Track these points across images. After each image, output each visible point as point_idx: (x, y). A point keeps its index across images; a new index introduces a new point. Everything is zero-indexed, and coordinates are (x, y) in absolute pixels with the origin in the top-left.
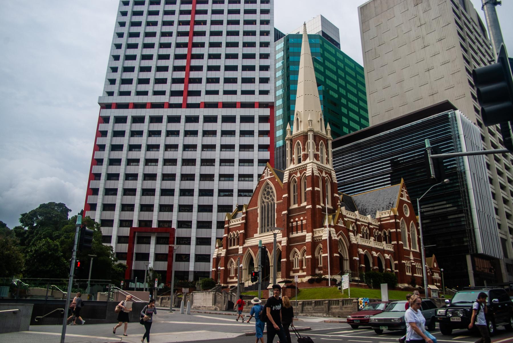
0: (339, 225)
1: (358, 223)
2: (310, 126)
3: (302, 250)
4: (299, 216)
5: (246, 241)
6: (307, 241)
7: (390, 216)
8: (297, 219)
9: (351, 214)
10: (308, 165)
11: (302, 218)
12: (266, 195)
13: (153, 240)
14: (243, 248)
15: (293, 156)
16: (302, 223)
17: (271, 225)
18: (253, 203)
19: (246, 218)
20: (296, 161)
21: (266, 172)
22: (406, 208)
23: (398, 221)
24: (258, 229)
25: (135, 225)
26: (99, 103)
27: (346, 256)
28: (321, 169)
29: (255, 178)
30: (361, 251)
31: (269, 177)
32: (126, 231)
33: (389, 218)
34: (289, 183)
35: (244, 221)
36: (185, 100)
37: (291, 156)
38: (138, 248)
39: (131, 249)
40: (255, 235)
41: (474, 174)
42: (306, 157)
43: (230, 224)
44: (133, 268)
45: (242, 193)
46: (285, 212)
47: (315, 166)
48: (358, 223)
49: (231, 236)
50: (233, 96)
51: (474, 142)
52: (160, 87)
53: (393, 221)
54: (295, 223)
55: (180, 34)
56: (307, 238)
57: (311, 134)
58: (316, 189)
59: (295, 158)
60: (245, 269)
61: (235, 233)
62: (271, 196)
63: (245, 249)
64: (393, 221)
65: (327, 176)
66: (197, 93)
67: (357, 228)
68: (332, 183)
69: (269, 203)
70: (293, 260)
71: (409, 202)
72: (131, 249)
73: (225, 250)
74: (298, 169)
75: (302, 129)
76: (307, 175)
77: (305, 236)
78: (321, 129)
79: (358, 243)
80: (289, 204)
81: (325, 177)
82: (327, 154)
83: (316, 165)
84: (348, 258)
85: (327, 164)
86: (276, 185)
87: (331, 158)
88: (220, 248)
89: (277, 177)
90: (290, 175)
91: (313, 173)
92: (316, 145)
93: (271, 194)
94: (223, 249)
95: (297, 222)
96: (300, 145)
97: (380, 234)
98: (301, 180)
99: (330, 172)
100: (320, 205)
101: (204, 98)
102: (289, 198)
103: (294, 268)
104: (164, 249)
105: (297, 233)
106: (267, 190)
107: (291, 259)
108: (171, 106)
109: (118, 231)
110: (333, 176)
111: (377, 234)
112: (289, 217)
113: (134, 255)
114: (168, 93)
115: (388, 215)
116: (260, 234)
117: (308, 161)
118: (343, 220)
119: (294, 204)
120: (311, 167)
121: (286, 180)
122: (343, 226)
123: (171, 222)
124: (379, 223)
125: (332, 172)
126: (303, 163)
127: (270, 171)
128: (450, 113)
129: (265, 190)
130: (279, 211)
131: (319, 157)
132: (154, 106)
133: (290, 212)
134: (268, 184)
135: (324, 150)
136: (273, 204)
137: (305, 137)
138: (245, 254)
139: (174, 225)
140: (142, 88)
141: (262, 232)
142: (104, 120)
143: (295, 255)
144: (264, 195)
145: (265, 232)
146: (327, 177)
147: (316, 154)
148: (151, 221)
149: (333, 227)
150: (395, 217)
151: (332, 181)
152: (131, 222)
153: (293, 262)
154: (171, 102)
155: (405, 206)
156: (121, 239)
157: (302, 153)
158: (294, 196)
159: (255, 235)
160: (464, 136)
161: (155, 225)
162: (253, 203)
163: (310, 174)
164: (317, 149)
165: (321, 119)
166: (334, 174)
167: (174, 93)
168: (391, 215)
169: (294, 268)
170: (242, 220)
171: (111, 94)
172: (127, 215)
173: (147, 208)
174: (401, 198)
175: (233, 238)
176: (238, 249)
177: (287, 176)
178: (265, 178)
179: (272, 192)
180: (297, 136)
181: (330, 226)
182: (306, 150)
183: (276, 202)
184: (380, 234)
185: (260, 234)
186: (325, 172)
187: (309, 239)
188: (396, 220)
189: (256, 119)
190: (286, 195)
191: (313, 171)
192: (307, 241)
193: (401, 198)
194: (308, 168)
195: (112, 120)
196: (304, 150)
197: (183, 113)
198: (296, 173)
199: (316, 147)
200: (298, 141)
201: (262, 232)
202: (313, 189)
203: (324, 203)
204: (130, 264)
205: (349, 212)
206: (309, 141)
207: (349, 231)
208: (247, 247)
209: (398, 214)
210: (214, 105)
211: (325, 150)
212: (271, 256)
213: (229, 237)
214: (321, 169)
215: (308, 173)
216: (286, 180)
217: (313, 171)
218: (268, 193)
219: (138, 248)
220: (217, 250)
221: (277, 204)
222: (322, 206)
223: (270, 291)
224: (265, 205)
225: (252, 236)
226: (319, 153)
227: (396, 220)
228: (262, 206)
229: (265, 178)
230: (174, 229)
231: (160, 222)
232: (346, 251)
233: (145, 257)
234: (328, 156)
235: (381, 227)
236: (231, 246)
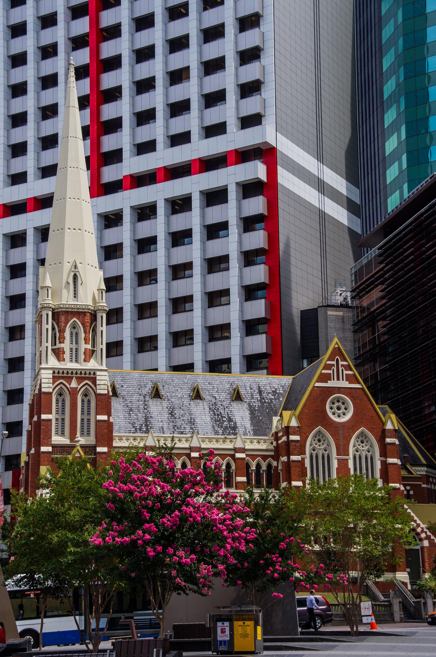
2: (50, 298)
65: (87, 384)
92: (59, 331)
99: (94, 374)
131: (64, 353)
147: (59, 349)
164: (59, 339)
184: (277, 467)
211: (83, 335)
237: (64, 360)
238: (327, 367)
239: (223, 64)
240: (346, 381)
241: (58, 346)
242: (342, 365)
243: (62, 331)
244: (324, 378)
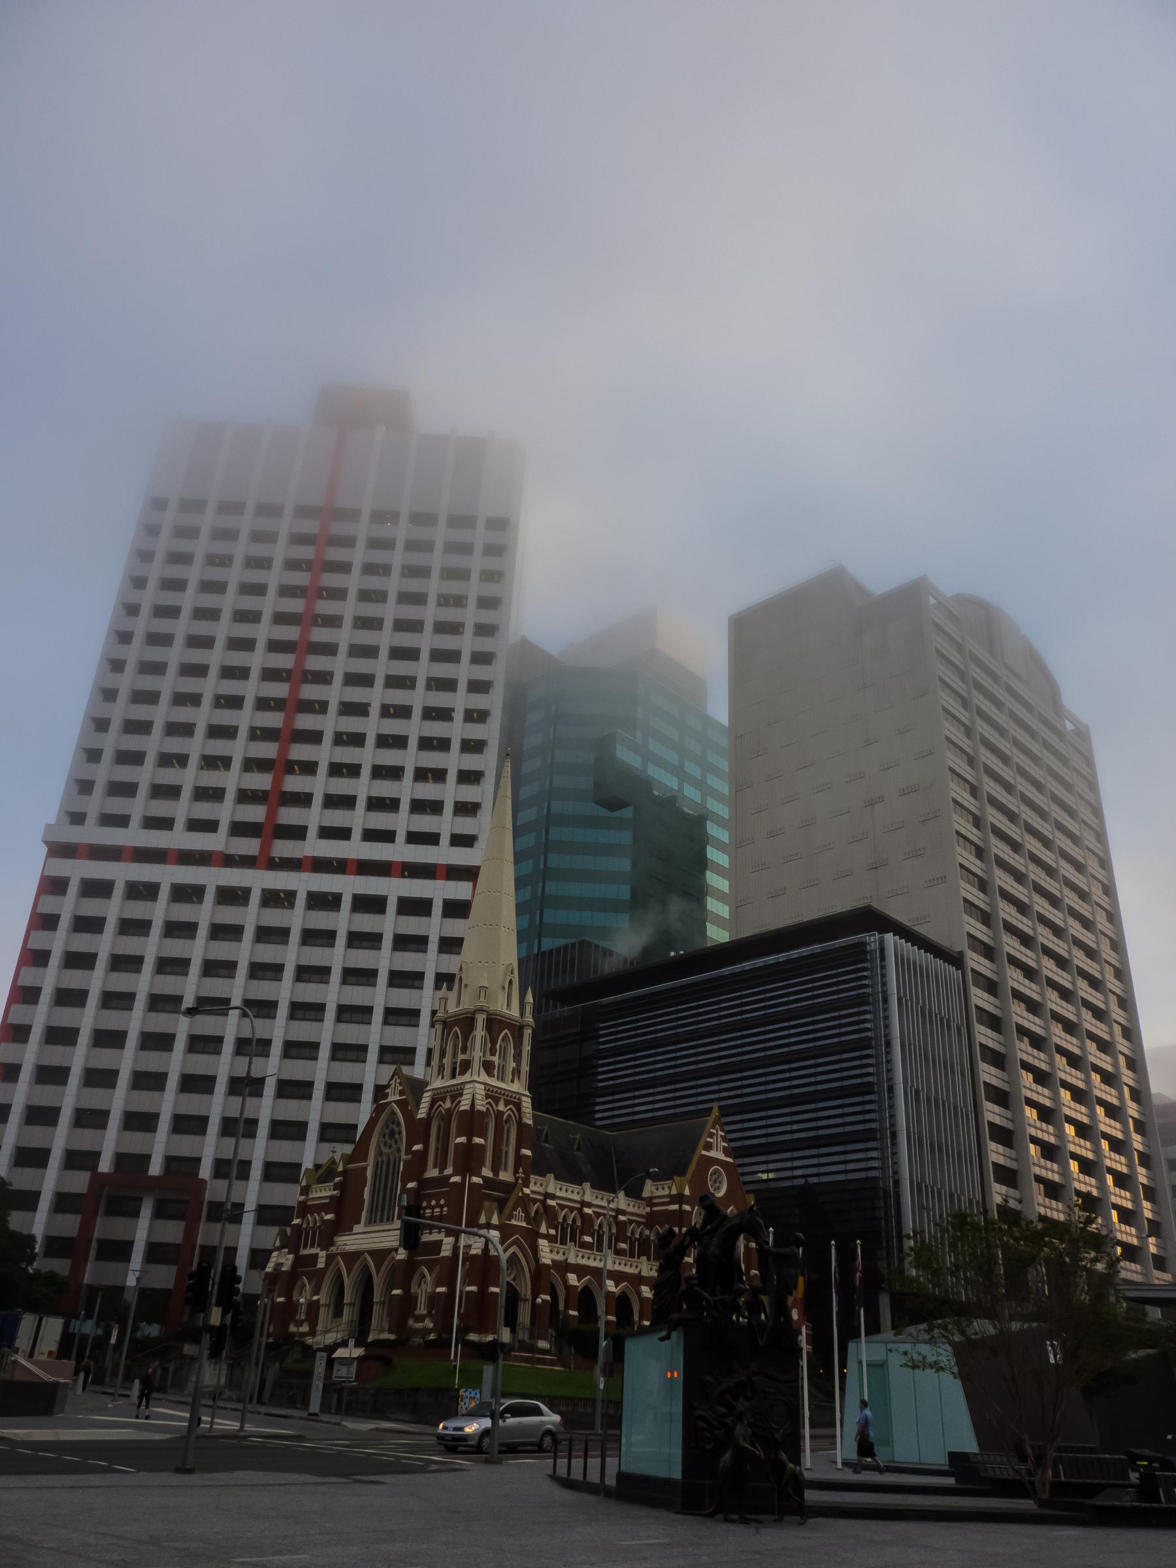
0: (513, 1222)
1: (587, 1210)
2: (482, 999)
4: (437, 1197)
5: (336, 1239)
6: (443, 1254)
7: (669, 1196)
8: (433, 1203)
9: (570, 1189)
10: (467, 1086)
11: (442, 1202)
12: (387, 1137)
13: (146, 1211)
14: (327, 1255)
15: (445, 1061)
16: (441, 1212)
17: (390, 1205)
18: (360, 1153)
20: (447, 1071)
21: (393, 1086)
22: (720, 1175)
23: (687, 1208)
24: (364, 1214)
25: (105, 1165)
26: (46, 842)
27: (526, 1290)
28: (493, 1095)
29: (367, 1095)
30: (572, 1279)
31: (397, 1098)
32: (79, 1182)
33: (668, 1200)
34: (428, 1121)
36: (266, 847)
37: (441, 1059)
38: (106, 1228)
39: (87, 1227)
40: (357, 1228)
41: (917, 1093)
42: (466, 1066)
43: (311, 1196)
44: (85, 1281)
45: (330, 1132)
46: (411, 1185)
47: (480, 1090)
48: (587, 1210)
49: (309, 1224)
50: (385, 845)
51: (935, 1008)
52: (205, 810)
53: (675, 1207)
54: (430, 1211)
55: (270, 675)
56: (443, 1247)
57: (481, 1019)
58: (477, 1140)
59: (446, 1066)
60: (326, 1305)
61: (317, 1218)
62: (396, 1142)
63: (330, 1259)
64: (675, 1207)
65: (510, 1109)
66: (298, 832)
67: (582, 1223)
68: (521, 1125)
69: (391, 1158)
70: (418, 1293)
71: (730, 1160)
72: (87, 1227)
73: (291, 1257)
74: (448, 1092)
75: (467, 1004)
76: (461, 1109)
77: (440, 1243)
78: (509, 1005)
79: (567, 1260)
80: (424, 1168)
81: (502, 1113)
82: (518, 1057)
83: (482, 1087)
84: (529, 1295)
85: (512, 1081)
86: (409, 1116)
87: (525, 1068)
88: (283, 1250)
90: (433, 1102)
91: (473, 1105)
92: (491, 1042)
93: (397, 1136)
94: (289, 1253)
95: (433, 1208)
96: (458, 1038)
97: (648, 1237)
98: (451, 1116)
99: (519, 1099)
100: (479, 1175)
101: (314, 847)
102: (424, 1154)
103: (417, 1312)
104: (172, 1232)
105: (430, 1233)
106: (391, 1126)
107: (412, 1291)
108: (229, 861)
109: (59, 1181)
110: (523, 1109)
111: (641, 1234)
112: (417, 1194)
113: (94, 1245)
114: (224, 828)
115: (666, 1192)
116: (366, 1225)
117: (467, 1077)
118: (526, 1211)
119: (435, 1166)
120: (470, 1091)
121: (422, 1113)
122: (524, 1224)
123: (197, 1161)
124: (648, 1209)
125: (524, 1098)
126: (459, 1080)
127: (400, 1084)
128: (872, 939)
130: (405, 1182)
131: (494, 1068)
132: (187, 858)
133: (423, 1183)
134: (393, 1113)
135: (511, 1051)
136: (397, 1160)
137: (466, 1022)
138: (331, 1268)
139: (205, 1172)
140: (161, 808)
141: (370, 1223)
142: (53, 886)
143: (422, 1283)
144: (384, 1136)
145: (375, 1222)
146: (509, 1112)
148: (146, 1158)
149: (495, 1228)
150: (679, 1198)
151: (520, 1119)
152: (96, 1156)
153: (416, 1298)
154: (232, 851)
155: (716, 1172)
156: (63, 1202)
157: (461, 1057)
158: (437, 1149)
160: (900, 1000)
161: (155, 1168)
162: (360, 1153)
163: (467, 1108)
164: (491, 1050)
165: (511, 982)
166: (527, 1104)
167: (240, 829)
168: (672, 1193)
169: (417, 1312)
171: (77, 818)
172: (85, 1140)
173: (139, 1122)
174: (704, 1153)
175: (312, 1228)
176: (316, 1256)
177: (426, 1105)
178: (390, 1099)
179: (400, 1133)
180: (455, 1016)
181: (488, 1226)
182: (468, 1052)
183: (403, 1157)
184: (648, 1237)
185: (366, 1225)
186: (504, 1099)
187: (446, 1251)
188: (680, 1207)
189: (437, 908)
190: (417, 1147)
191: (473, 1101)
192: (443, 1254)
193: (704, 1153)
194: (465, 1092)
195: (73, 888)
196: (464, 1050)
197: (258, 880)
198: (444, 1100)
199: (489, 1045)
200: (457, 1028)
201: (370, 1222)
202: (470, 1140)
203: (495, 1169)
204: (78, 1270)
205: (565, 1185)
206: (475, 1033)
207: (539, 1235)
209: (687, 1192)
210: (339, 866)
211: (513, 1051)
212: (378, 1281)
213: (304, 1226)
214: (493, 1095)
215: (465, 1105)
216: (422, 1113)
217: (473, 1101)
219: (106, 1228)
221: (406, 1162)
222: (484, 1179)
223: (336, 1361)
224: (383, 1161)
225: (348, 1230)
226: (495, 1059)
227: (680, 1207)
228: (378, 1162)
229: (390, 1099)
230: (203, 1181)
231: (169, 1161)
232: (525, 1280)
233: (119, 1251)
234: (519, 1064)
235: (651, 1220)
236: (305, 1247)
237: (494, 1076)
238: (711, 1135)
239: (401, 773)
240: (723, 1152)
241: (489, 1058)
242: (721, 1136)
243: (494, 1042)
244: (708, 1147)
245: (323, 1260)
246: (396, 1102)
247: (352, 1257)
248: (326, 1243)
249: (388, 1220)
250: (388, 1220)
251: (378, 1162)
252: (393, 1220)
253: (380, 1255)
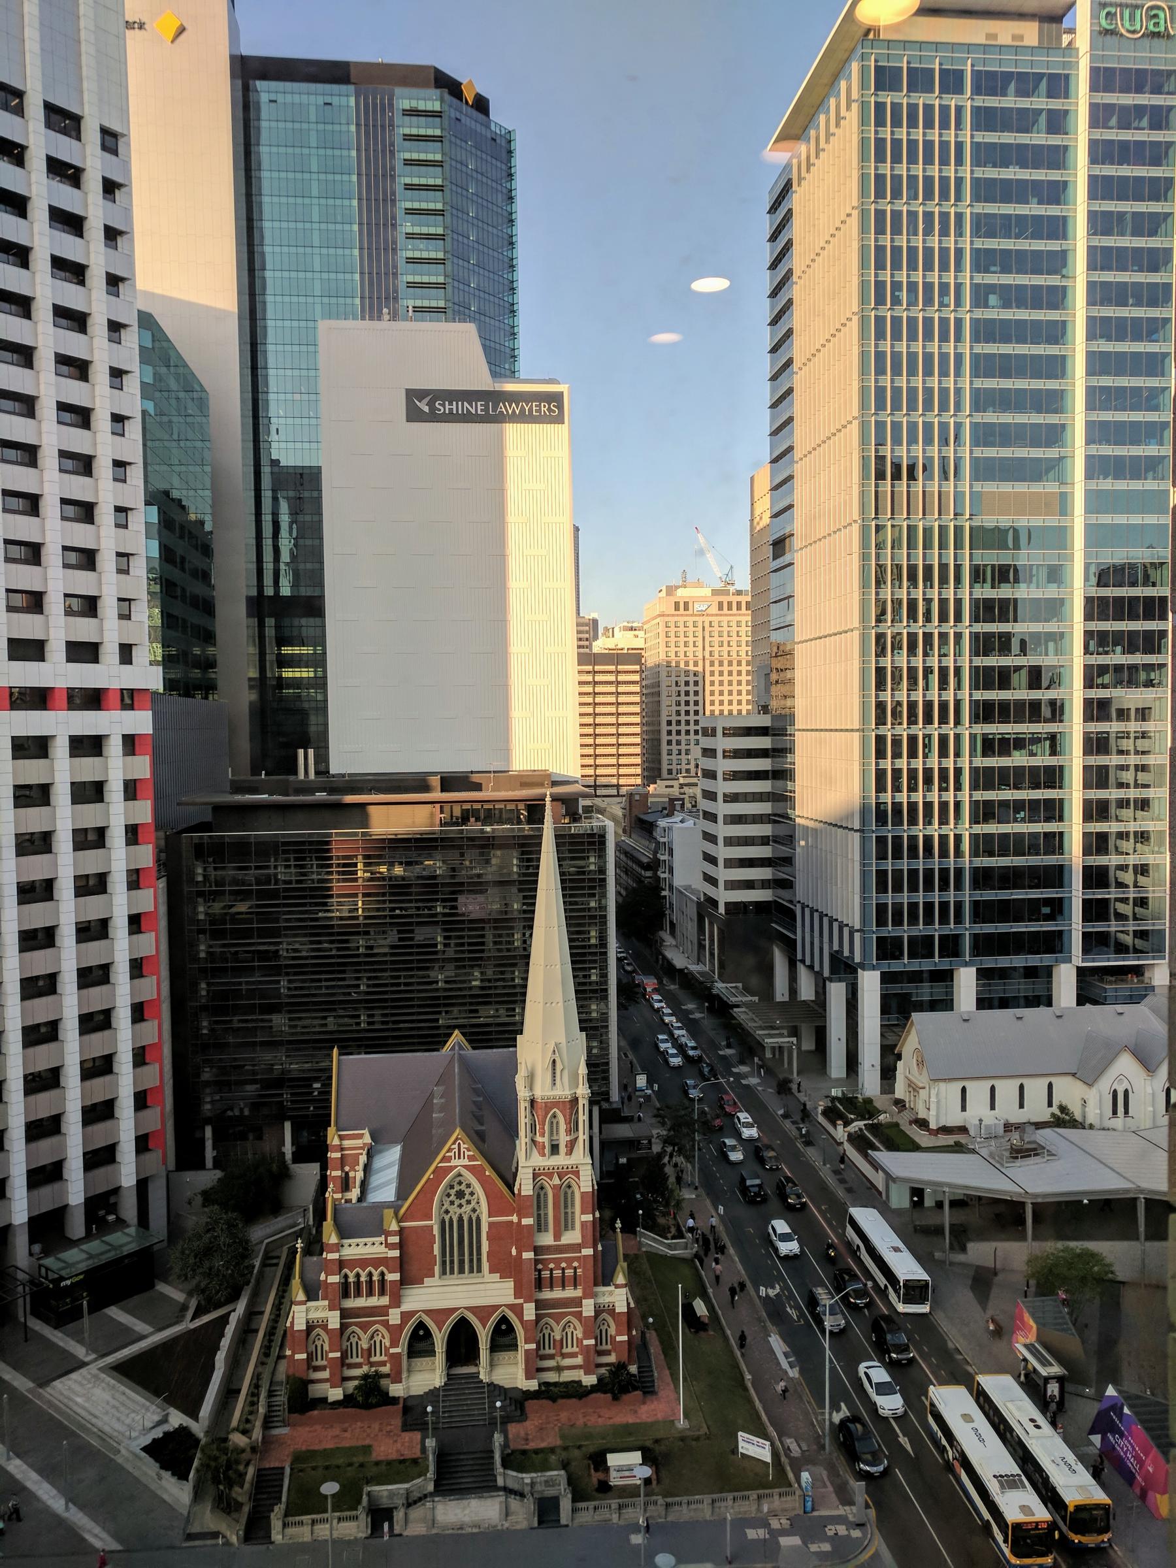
3: (563, 1322)
17: (471, 1261)
19: (401, 1246)
31: (466, 1162)
35: (396, 1253)
63: (406, 1316)
89: (486, 1166)
90: (535, 1176)
127: (469, 1150)
129: (452, 1187)
134: (460, 1175)
145: (452, 1272)
159: (426, 1280)
170: (390, 1246)
178: (453, 1163)
179: (472, 1194)
208: (413, 1313)
218: (460, 1194)
220: (303, 1308)
221: (491, 1225)
245: (399, 1317)
246: (465, 1167)
247: (439, 1315)
248: (396, 1302)
249: (471, 1271)
250: (471, 1271)
251: (443, 1222)
252: (479, 1271)
253: (483, 1312)
